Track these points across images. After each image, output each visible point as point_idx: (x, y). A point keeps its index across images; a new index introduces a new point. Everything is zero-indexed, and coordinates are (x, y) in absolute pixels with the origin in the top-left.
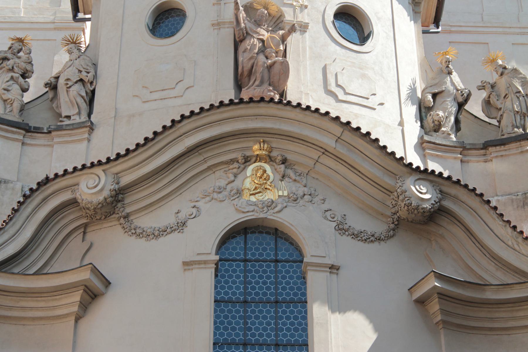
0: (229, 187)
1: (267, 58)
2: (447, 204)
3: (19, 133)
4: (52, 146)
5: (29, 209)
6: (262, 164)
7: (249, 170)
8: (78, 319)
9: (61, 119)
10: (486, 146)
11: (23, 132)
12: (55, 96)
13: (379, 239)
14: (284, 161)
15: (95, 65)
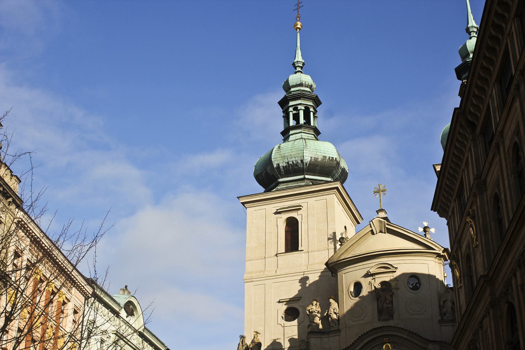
1: (387, 304)
3: (320, 335)
4: (329, 337)
6: (387, 344)
9: (331, 328)
11: (321, 334)
14: (394, 342)
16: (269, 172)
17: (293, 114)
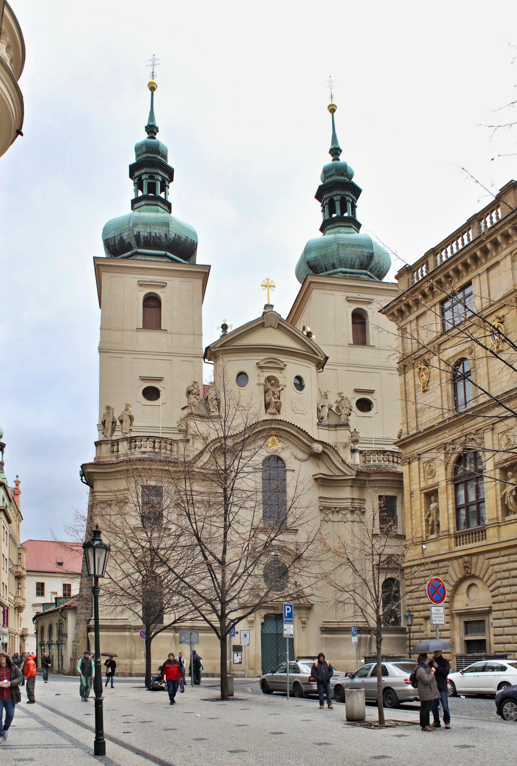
2: (325, 450)
7: (270, 439)
10: (336, 426)
13: (305, 460)
14: (280, 436)
16: (125, 238)
17: (149, 184)
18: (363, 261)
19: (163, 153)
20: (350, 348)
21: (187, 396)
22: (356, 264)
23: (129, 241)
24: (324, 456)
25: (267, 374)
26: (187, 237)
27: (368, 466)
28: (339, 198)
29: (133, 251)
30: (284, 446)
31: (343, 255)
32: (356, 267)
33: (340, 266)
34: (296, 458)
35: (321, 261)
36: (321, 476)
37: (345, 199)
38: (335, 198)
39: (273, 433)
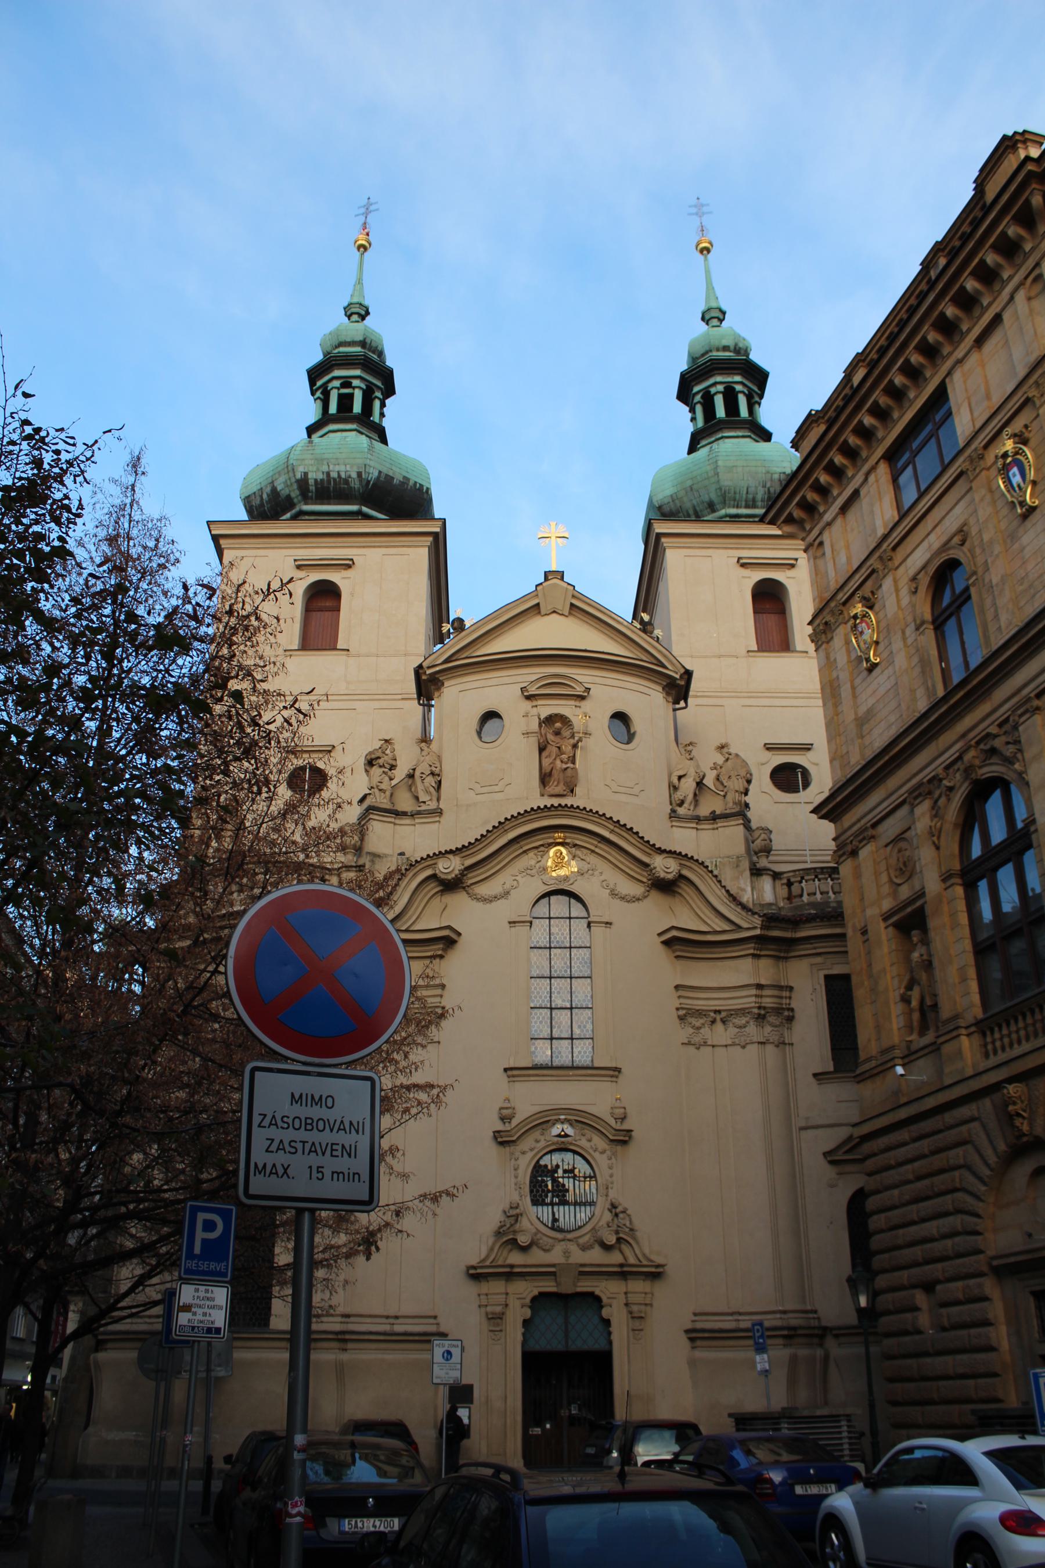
0: (538, 865)
2: (685, 872)
5: (405, 882)
7: (552, 852)
8: (441, 957)
10: (714, 817)
12: (414, 782)
13: (638, 899)
14: (575, 845)
15: (439, 758)
16: (279, 488)
17: (341, 397)
18: (772, 490)
19: (373, 344)
20: (751, 659)
21: (366, 771)
22: (759, 497)
23: (286, 492)
24: (686, 888)
25: (547, 708)
26: (404, 477)
27: (796, 908)
28: (720, 388)
29: (294, 511)
30: (586, 867)
31: (726, 483)
32: (759, 504)
33: (724, 504)
34: (613, 894)
35: (685, 499)
36: (674, 933)
37: (734, 389)
38: (713, 390)
39: (559, 836)
